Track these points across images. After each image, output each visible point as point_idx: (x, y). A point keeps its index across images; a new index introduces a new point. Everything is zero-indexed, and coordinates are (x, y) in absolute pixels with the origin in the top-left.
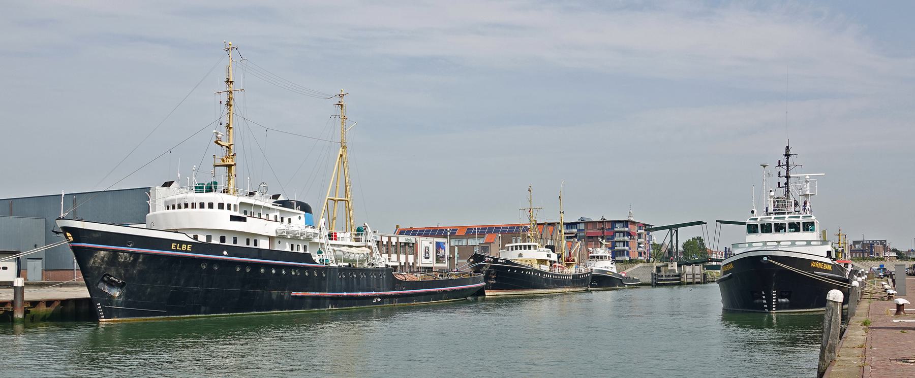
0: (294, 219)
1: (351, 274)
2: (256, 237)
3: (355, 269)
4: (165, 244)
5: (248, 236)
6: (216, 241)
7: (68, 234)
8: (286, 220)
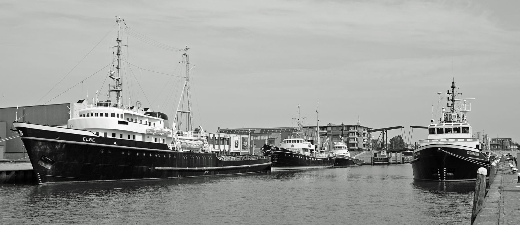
0: (157, 123)
1: (192, 157)
2: (134, 134)
3: (194, 154)
5: (129, 133)
6: (110, 136)
7: (20, 131)
8: (152, 124)
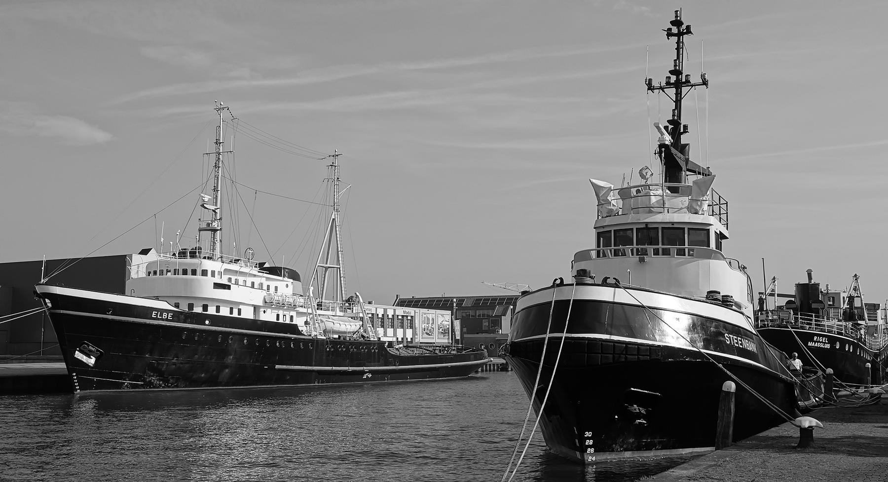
4: (146, 312)
6: (198, 310)
7: (47, 301)
